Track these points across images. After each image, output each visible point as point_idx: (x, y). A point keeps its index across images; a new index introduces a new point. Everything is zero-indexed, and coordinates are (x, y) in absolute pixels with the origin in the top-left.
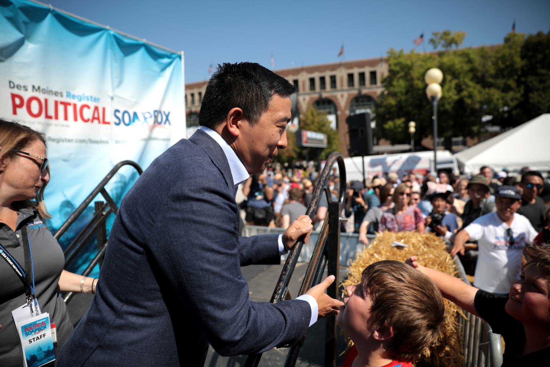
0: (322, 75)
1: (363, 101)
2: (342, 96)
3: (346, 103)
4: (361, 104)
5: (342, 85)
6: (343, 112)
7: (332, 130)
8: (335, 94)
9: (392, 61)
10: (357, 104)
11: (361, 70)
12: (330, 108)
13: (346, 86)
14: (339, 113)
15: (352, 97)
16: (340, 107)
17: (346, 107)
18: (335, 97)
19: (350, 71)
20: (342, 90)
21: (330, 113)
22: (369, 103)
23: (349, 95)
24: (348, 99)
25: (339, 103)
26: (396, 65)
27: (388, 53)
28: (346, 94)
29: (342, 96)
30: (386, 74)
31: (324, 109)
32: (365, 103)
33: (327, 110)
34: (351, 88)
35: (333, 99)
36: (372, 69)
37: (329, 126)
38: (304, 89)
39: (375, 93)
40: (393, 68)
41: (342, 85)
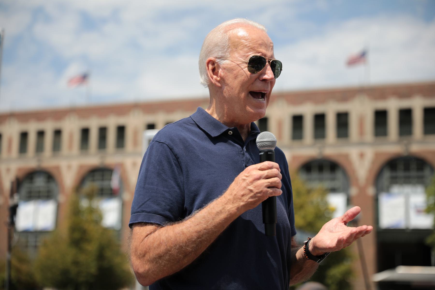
0: (319, 109)
1: (407, 168)
2: (362, 156)
4: (400, 173)
10: (394, 174)
11: (405, 104)
12: (333, 179)
15: (383, 160)
16: (357, 180)
18: (347, 156)
19: (381, 105)
20: (361, 143)
21: (334, 190)
22: (420, 174)
23: (377, 155)
24: (373, 162)
29: (362, 156)
31: (321, 180)
32: (413, 173)
33: (327, 184)
35: (341, 161)
41: (362, 132)
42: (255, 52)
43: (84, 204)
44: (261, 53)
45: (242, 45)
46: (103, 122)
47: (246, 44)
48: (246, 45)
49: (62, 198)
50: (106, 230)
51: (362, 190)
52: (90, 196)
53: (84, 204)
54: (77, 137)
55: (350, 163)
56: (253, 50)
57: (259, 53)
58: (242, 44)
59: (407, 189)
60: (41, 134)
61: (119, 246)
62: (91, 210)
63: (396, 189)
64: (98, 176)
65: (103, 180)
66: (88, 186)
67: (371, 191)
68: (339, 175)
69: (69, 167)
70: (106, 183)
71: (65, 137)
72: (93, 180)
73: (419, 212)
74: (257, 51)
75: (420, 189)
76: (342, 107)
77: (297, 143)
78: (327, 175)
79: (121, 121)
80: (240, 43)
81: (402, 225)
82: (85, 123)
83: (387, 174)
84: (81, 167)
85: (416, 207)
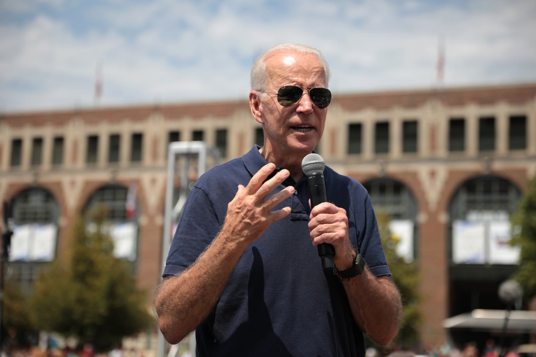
0: (382, 116)
1: (488, 191)
2: (433, 174)
3: (442, 193)
4: (480, 197)
7: (400, 261)
8: (413, 167)
11: (487, 111)
12: (397, 203)
14: (422, 218)
15: (458, 180)
16: (427, 204)
17: (439, 203)
18: (414, 175)
19: (457, 112)
20: (433, 159)
21: (398, 217)
23: (451, 174)
24: (447, 183)
25: (423, 193)
28: (442, 171)
29: (433, 174)
32: (495, 197)
33: (390, 209)
34: (457, 155)
35: (408, 180)
36: (516, 110)
37: (393, 251)
38: (333, 149)
39: (523, 172)
41: (433, 146)
42: (289, 81)
43: (91, 228)
44: (296, 82)
45: (276, 75)
46: (115, 128)
47: (280, 73)
48: (279, 75)
49: (63, 222)
50: (119, 261)
51: (433, 216)
52: (99, 220)
53: (91, 228)
54: (83, 147)
55: (419, 183)
56: (287, 80)
57: (294, 82)
58: (276, 74)
59: (488, 216)
60: (38, 142)
61: (134, 281)
62: (100, 238)
63: (473, 216)
64: (108, 194)
65: (114, 199)
66: (96, 207)
67: (443, 218)
68: (404, 197)
69: (73, 183)
70: (118, 204)
71: (68, 146)
72: (102, 200)
73: (501, 243)
74: (291, 81)
75: (503, 216)
76: (410, 114)
77: (354, 158)
78: (389, 197)
79: (138, 127)
80: (274, 73)
81: (481, 259)
82: (92, 130)
83: (463, 197)
84: (87, 183)
85: (497, 238)
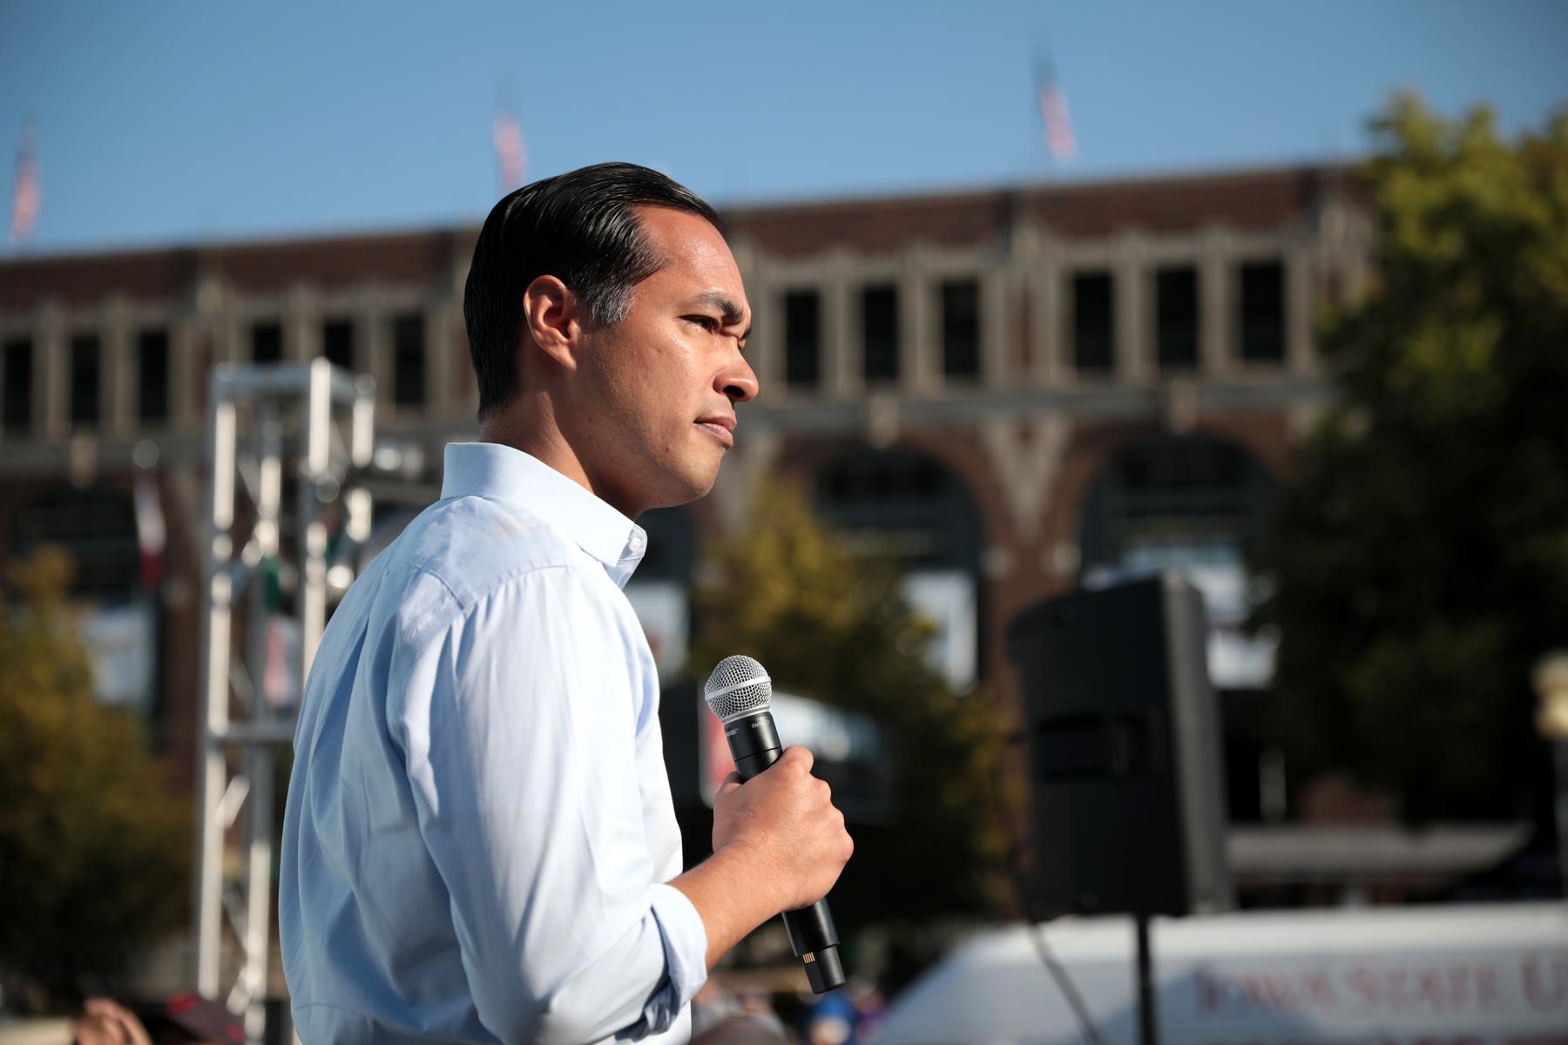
0: (878, 269)
2: (1026, 436)
5: (1025, 354)
6: (1031, 556)
9: (1406, 192)
11: (1174, 250)
13: (1053, 372)
14: (999, 562)
18: (973, 439)
19: (1091, 255)
26: (1437, 220)
27: (1378, 125)
29: (1026, 436)
30: (1360, 285)
36: (1257, 246)
39: (1278, 422)
40: (1412, 237)
41: (1025, 354)
